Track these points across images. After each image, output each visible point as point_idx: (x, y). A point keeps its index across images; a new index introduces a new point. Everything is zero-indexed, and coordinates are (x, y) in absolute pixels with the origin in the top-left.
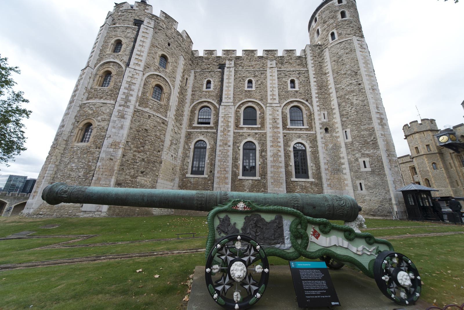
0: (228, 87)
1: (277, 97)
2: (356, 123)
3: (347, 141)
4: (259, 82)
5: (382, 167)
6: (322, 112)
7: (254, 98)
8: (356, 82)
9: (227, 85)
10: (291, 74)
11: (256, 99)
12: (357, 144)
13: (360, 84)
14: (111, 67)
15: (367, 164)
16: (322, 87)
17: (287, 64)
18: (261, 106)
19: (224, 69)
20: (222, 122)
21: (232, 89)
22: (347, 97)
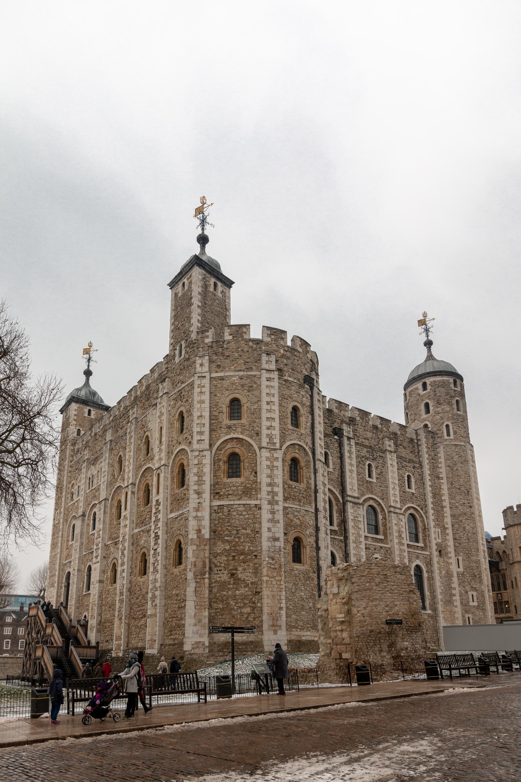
0: (351, 471)
1: (398, 499)
2: (467, 552)
3: (459, 570)
4: (379, 471)
5: (484, 603)
6: (437, 529)
7: (375, 495)
8: (469, 503)
9: (350, 468)
10: (407, 466)
11: (378, 497)
12: (467, 575)
13: (471, 507)
14: (297, 451)
15: (475, 598)
16: (437, 495)
17: (401, 447)
18: (382, 507)
19: (342, 437)
20: (353, 527)
21: (355, 475)
22: (460, 518)
